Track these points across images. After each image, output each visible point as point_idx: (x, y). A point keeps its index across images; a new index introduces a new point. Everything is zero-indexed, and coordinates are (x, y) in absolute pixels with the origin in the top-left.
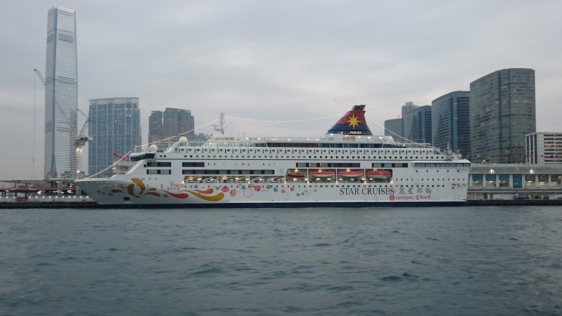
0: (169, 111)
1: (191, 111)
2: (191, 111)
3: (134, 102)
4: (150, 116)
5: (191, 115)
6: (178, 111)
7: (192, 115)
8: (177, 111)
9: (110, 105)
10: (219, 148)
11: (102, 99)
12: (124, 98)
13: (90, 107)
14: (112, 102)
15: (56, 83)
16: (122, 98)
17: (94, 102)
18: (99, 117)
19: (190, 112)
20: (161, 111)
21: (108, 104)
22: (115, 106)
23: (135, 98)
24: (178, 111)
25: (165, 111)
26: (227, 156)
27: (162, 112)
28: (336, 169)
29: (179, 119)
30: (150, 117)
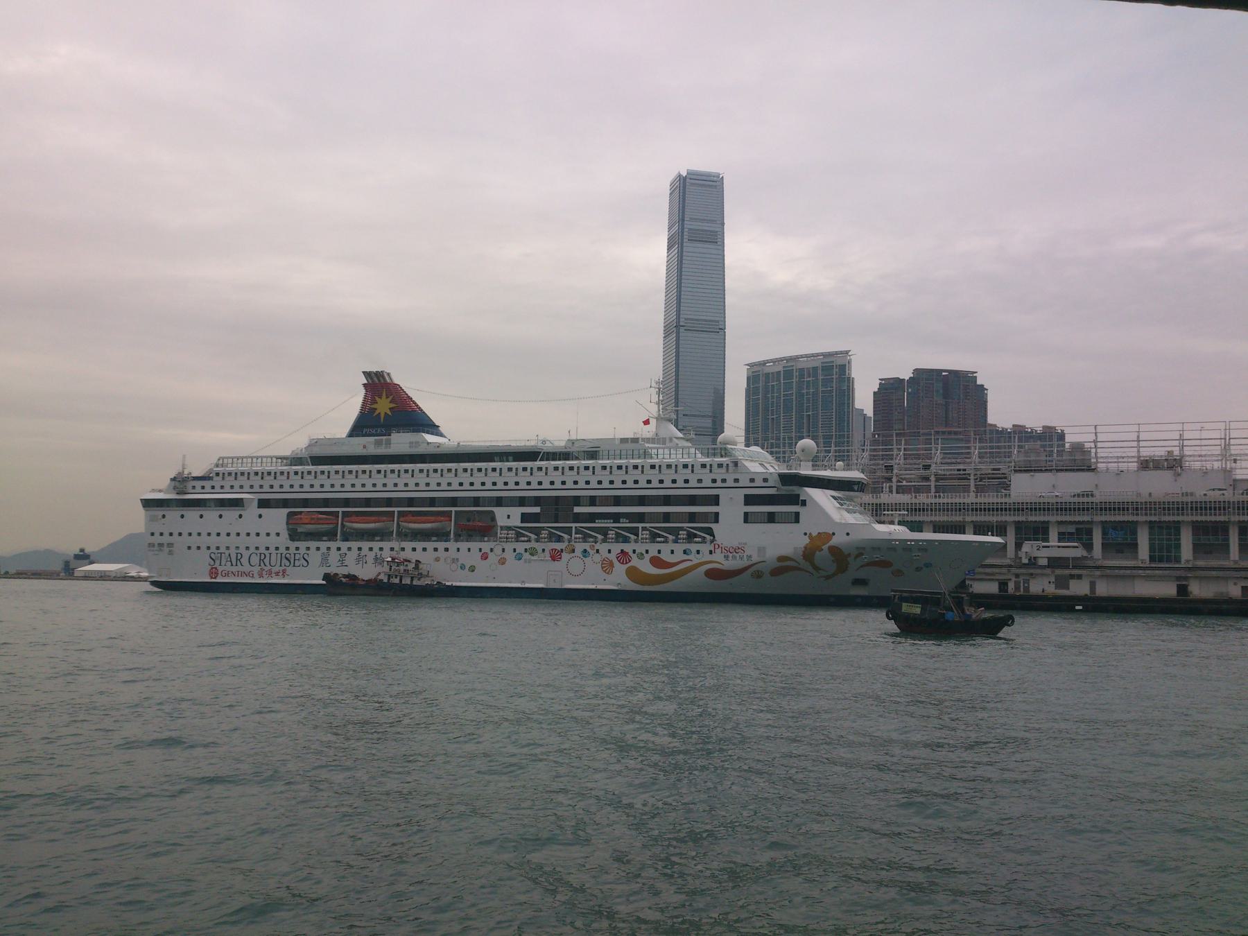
0: (922, 376)
1: (976, 372)
2: (976, 372)
3: (839, 361)
4: (876, 390)
5: (976, 381)
6: (944, 374)
7: (979, 382)
8: (941, 375)
9: (788, 373)
10: (632, 461)
11: (771, 361)
12: (818, 355)
13: (748, 378)
14: (793, 366)
15: (682, 330)
16: (813, 355)
17: (756, 369)
18: (801, 395)
19: (975, 375)
20: (901, 378)
21: (822, 366)
22: (837, 370)
23: (841, 353)
24: (944, 374)
25: (910, 378)
26: (702, 480)
27: (904, 379)
28: (394, 511)
29: (946, 395)
30: (874, 393)
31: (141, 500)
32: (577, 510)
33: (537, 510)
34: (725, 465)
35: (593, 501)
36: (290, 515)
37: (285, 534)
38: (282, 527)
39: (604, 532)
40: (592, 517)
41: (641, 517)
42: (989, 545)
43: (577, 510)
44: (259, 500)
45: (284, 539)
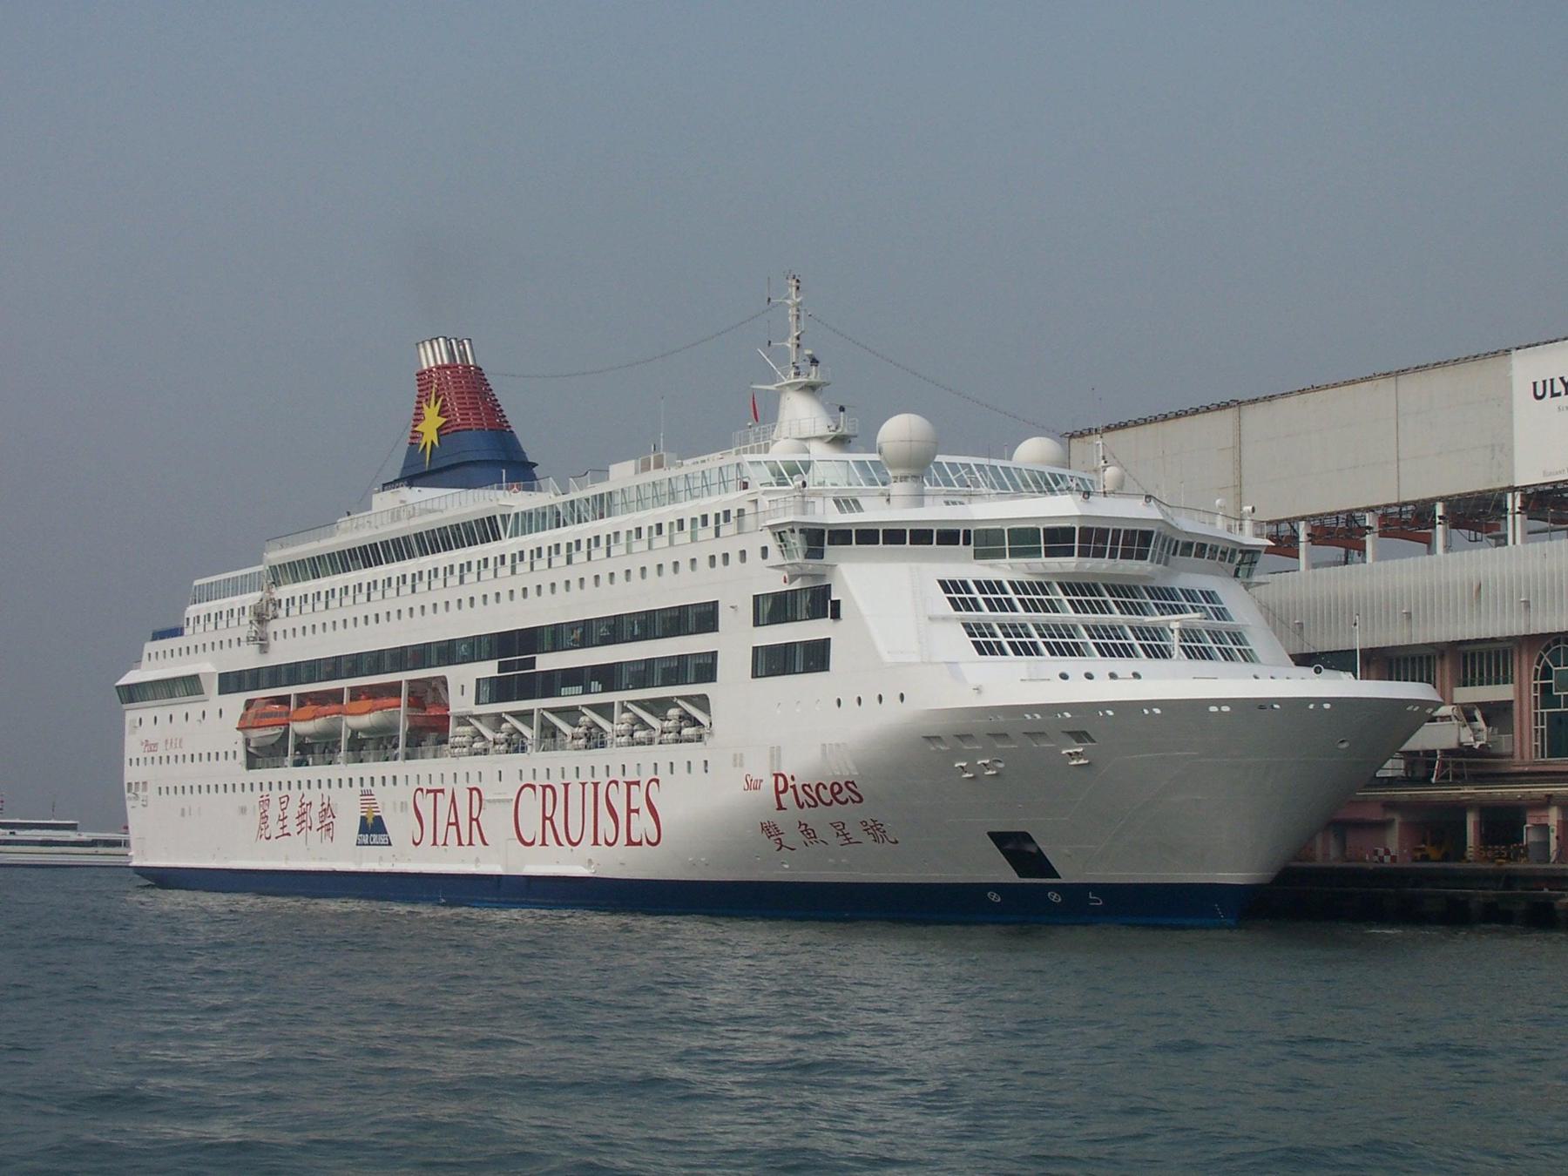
31: (117, 687)
32: (546, 662)
33: (489, 669)
34: (734, 513)
35: (555, 637)
36: (249, 704)
37: (242, 756)
38: (234, 741)
39: (570, 714)
40: (575, 677)
41: (609, 677)
42: (1311, 706)
43: (546, 662)
44: (220, 674)
45: (235, 769)
